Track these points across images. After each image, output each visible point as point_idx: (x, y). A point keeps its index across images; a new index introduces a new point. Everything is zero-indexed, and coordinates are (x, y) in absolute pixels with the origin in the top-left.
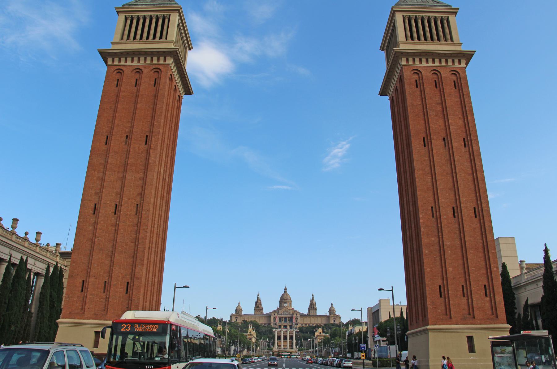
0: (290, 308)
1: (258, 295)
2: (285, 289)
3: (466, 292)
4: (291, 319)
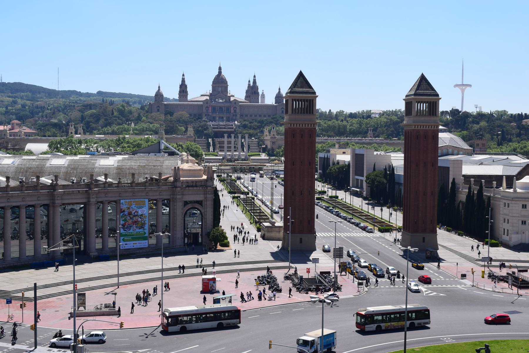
1: (183, 75)
4: (228, 109)
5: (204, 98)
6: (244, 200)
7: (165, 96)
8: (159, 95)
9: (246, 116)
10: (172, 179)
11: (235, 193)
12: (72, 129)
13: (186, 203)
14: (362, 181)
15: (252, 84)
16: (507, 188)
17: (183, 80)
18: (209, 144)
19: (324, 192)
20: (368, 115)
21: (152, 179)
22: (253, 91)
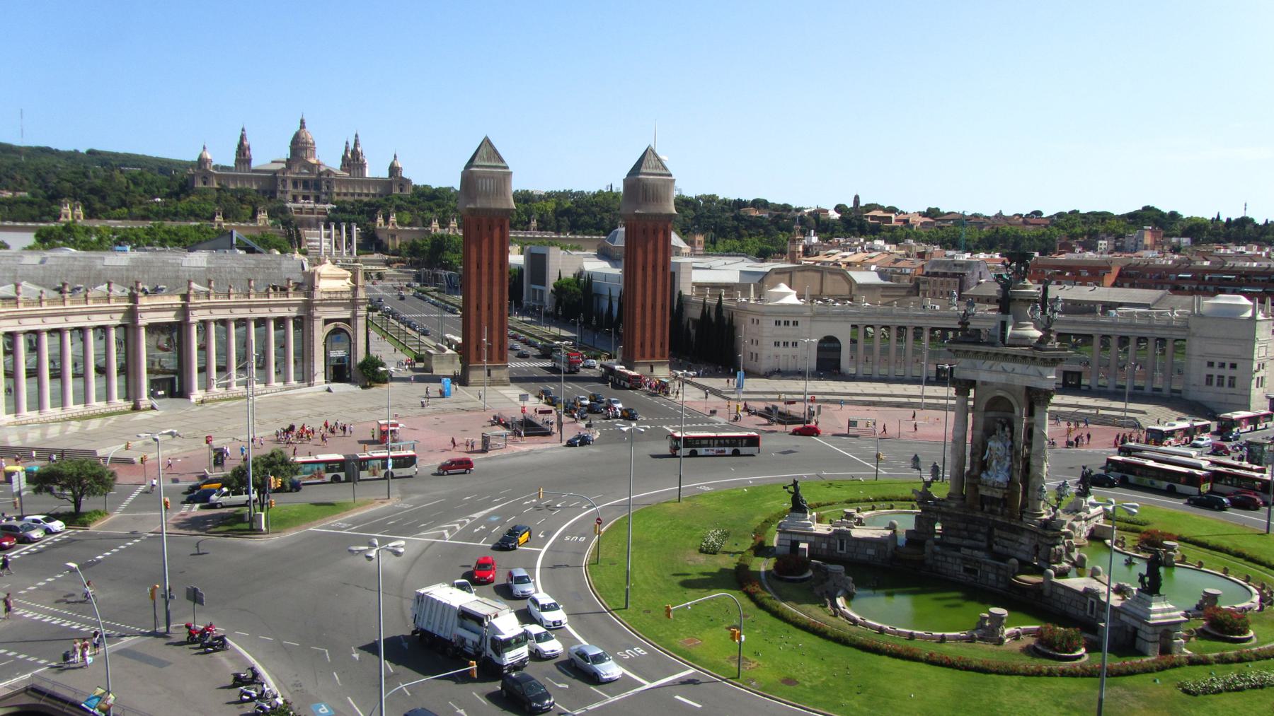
0: (313, 161)
2: (302, 122)
3: (653, 346)
4: (317, 185)
15: (351, 146)
22: (353, 160)
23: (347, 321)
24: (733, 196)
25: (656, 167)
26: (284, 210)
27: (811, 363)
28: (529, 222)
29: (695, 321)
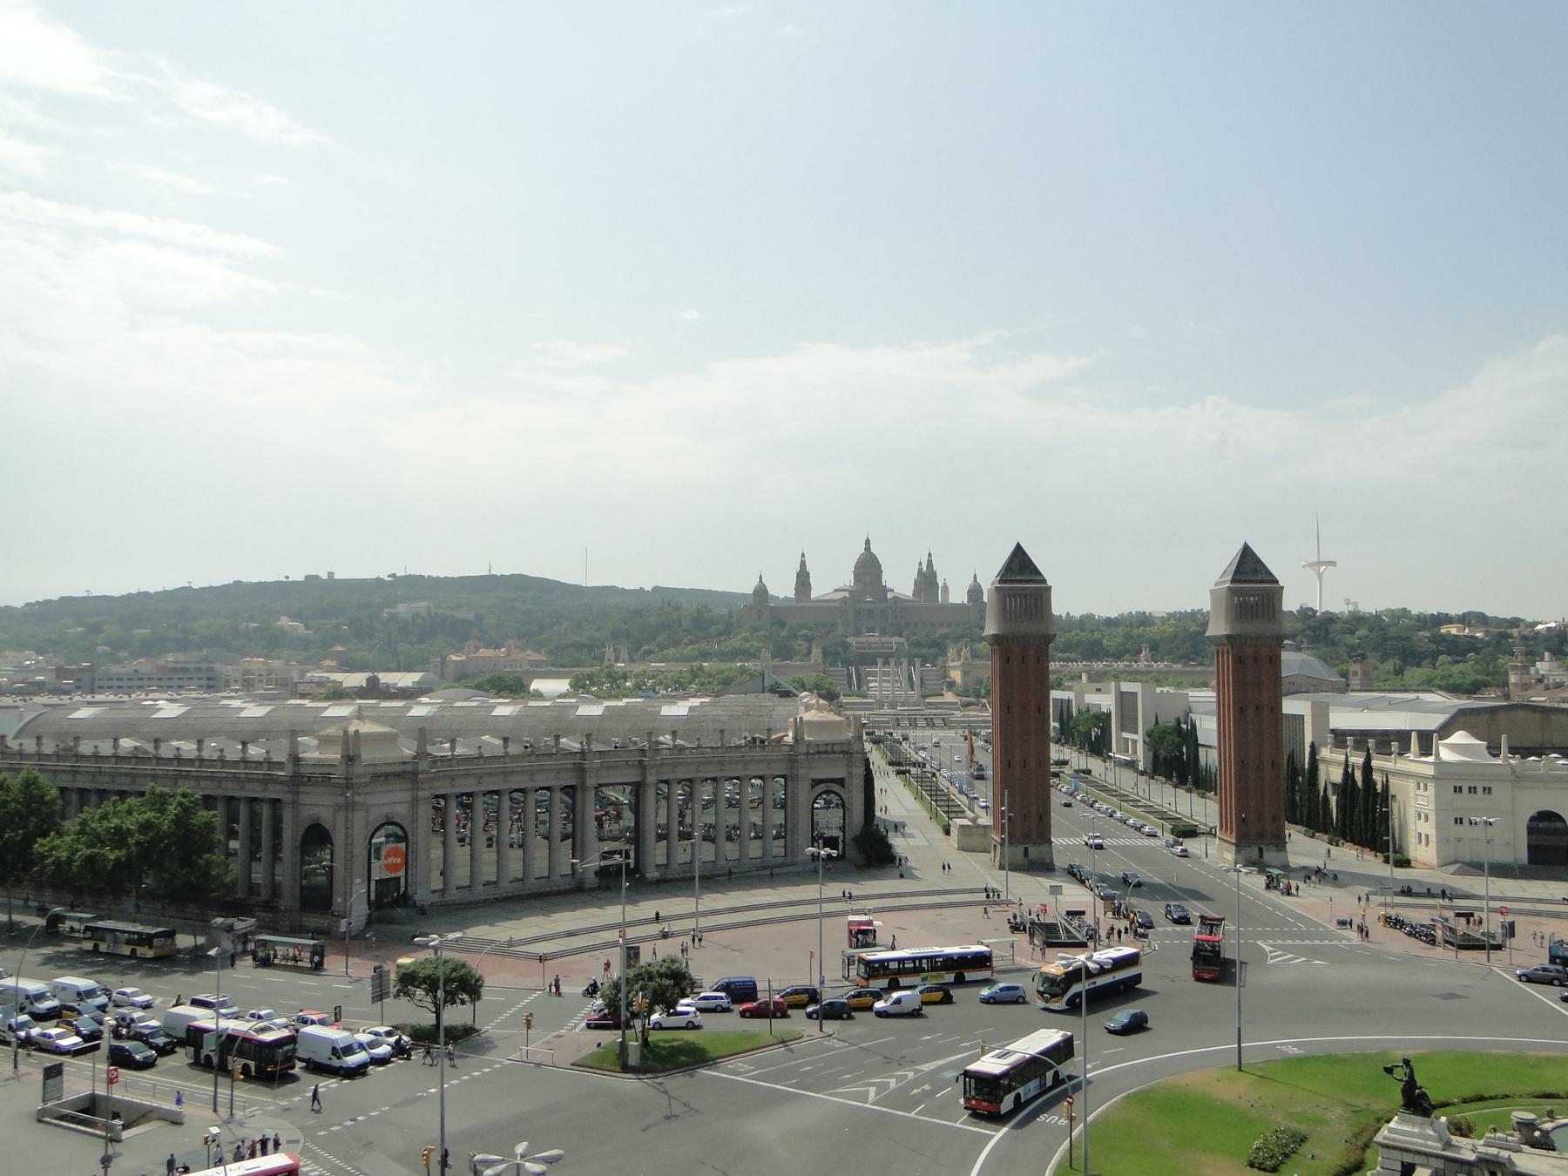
2: (868, 542)
5: (840, 595)
6: (917, 777)
7: (770, 592)
8: (761, 591)
9: (916, 625)
10: (789, 739)
11: (900, 764)
12: (609, 652)
13: (816, 782)
14: (1134, 742)
16: (1422, 755)
17: (803, 564)
18: (850, 676)
19: (1065, 763)
20: (1144, 620)
21: (754, 739)
22: (927, 580)
23: (841, 782)
24: (1432, 610)
25: (1255, 571)
26: (846, 646)
27: (1520, 853)
28: (1139, 652)
29: (1334, 785)
